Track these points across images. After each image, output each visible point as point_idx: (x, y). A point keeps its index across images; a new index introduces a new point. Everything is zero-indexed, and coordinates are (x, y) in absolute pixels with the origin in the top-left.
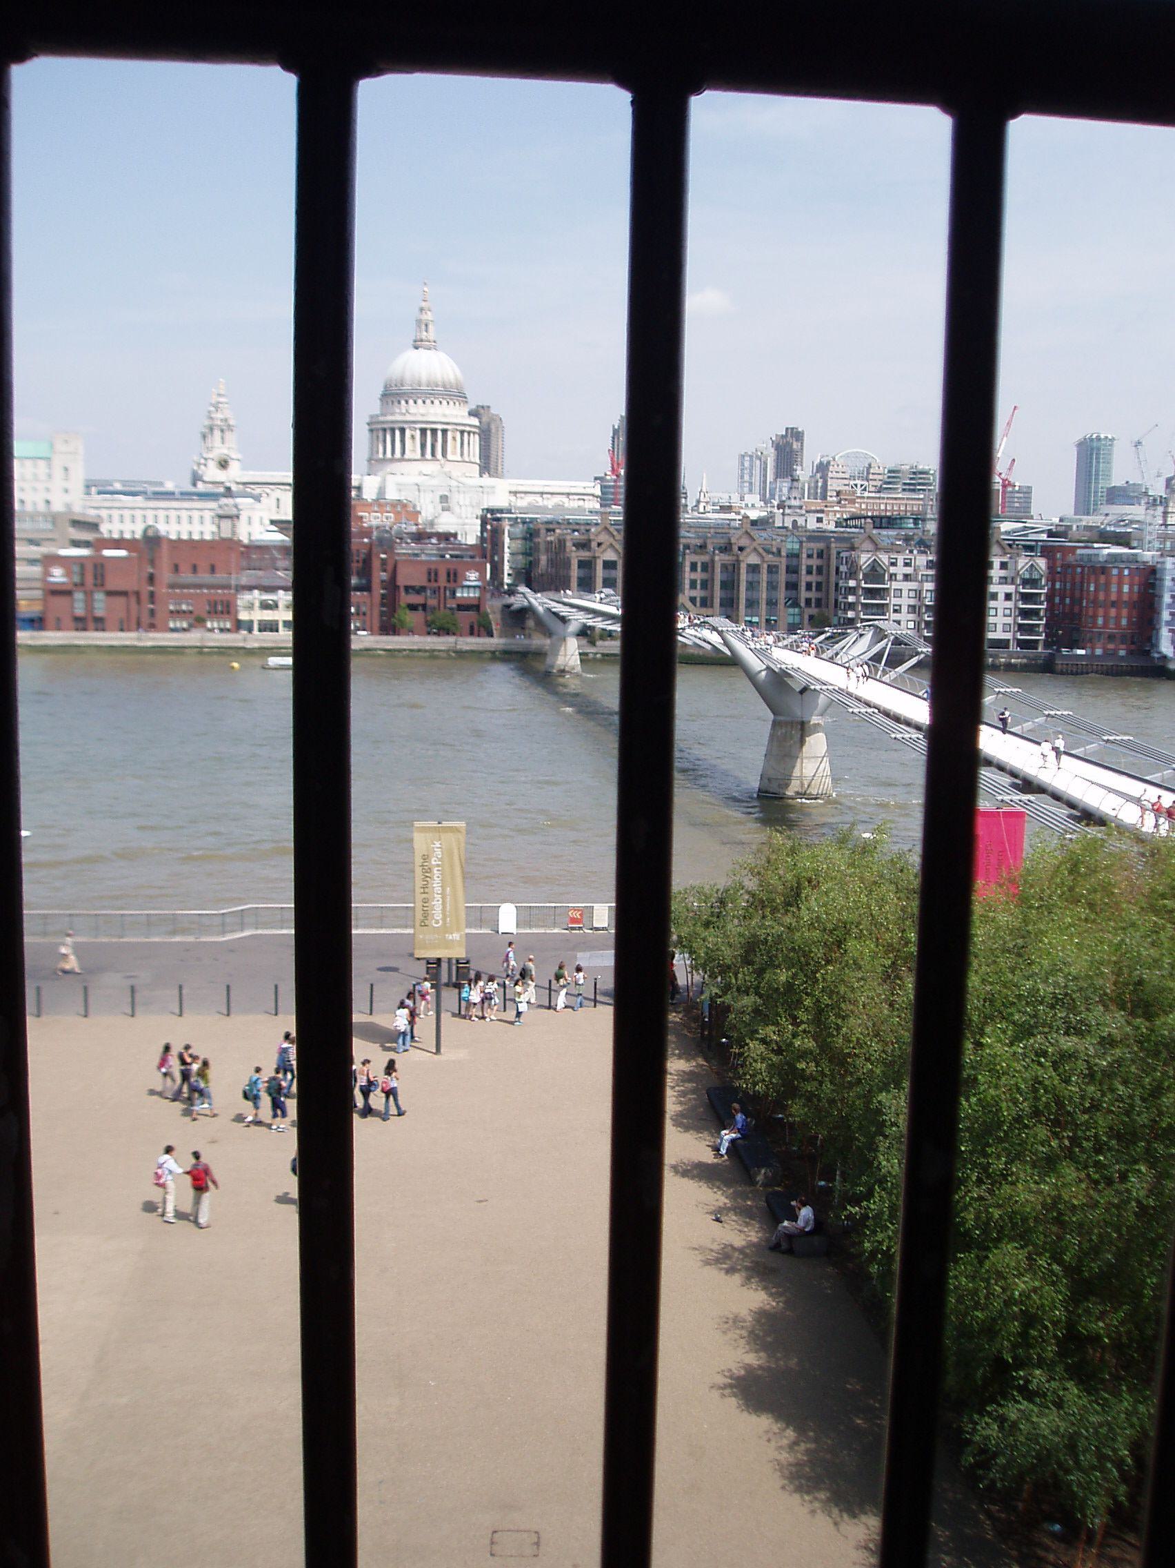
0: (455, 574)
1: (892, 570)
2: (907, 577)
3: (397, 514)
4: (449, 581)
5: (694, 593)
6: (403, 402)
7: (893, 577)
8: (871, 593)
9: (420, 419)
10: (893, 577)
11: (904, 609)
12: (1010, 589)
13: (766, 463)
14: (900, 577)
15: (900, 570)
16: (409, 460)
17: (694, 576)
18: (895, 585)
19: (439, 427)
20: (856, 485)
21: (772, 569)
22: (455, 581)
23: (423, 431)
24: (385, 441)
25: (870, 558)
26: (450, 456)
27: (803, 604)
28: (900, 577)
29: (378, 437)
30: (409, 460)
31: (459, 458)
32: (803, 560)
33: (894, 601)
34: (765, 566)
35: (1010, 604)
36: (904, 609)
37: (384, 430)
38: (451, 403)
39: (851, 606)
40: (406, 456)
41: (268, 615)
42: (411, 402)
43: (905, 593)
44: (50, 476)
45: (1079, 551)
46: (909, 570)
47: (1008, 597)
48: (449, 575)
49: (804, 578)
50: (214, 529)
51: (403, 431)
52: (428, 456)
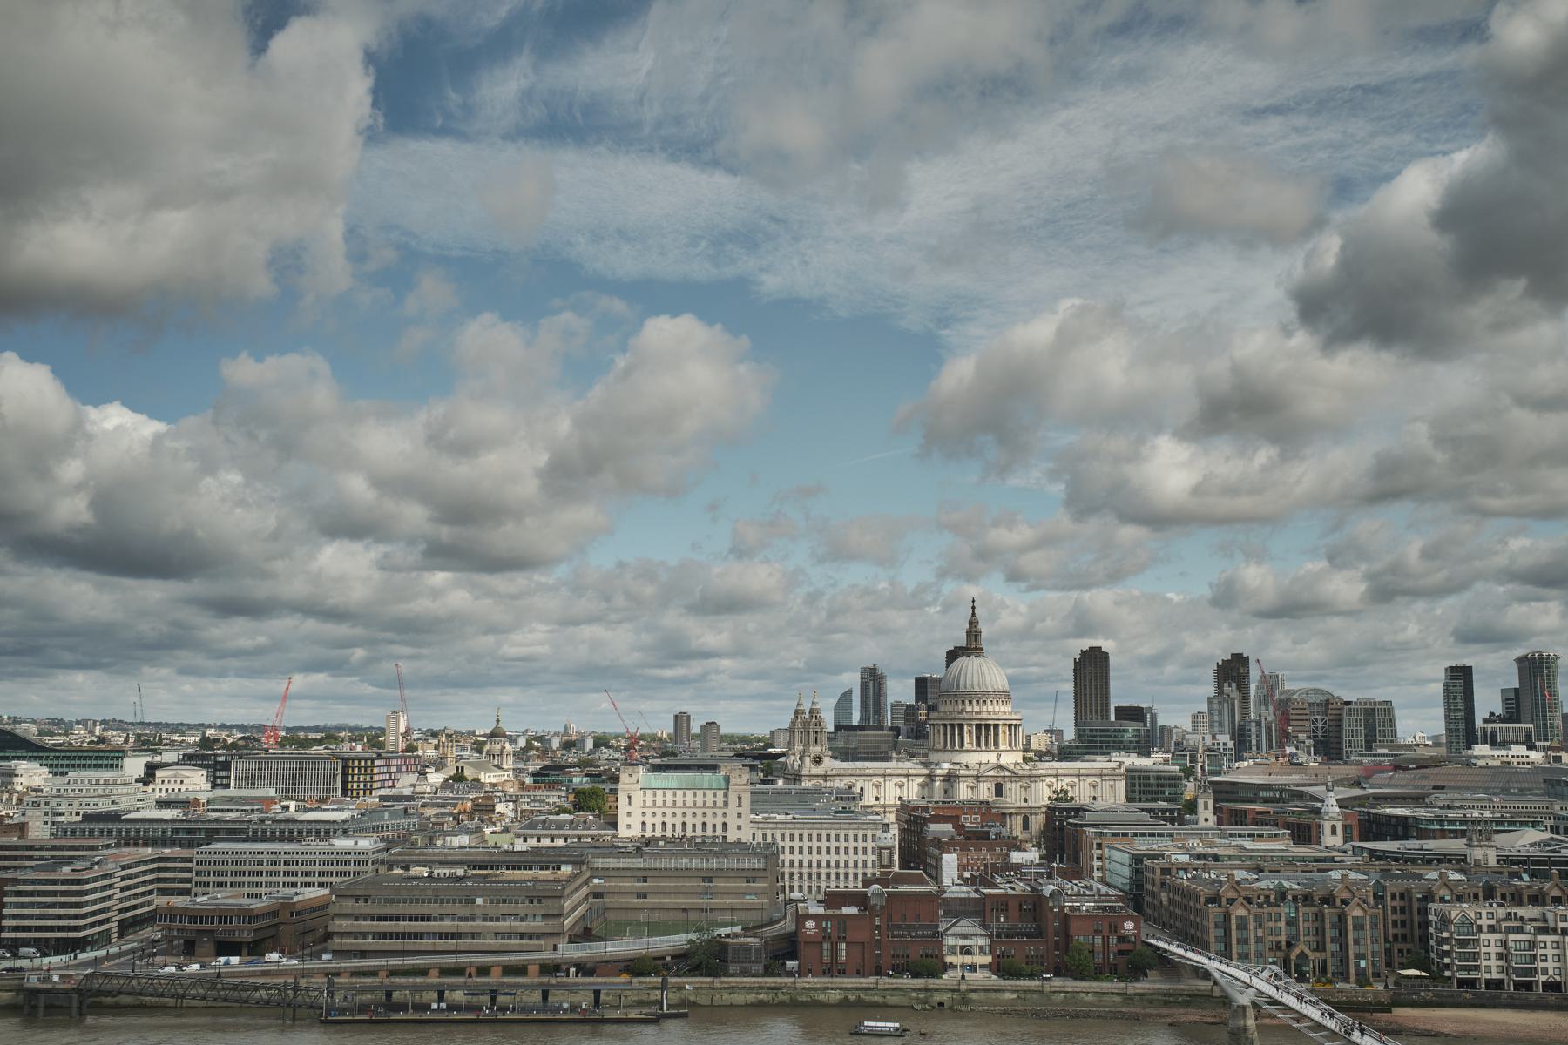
0: (1116, 927)
2: (1492, 929)
3: (983, 815)
4: (1110, 931)
5: (1307, 939)
6: (960, 702)
7: (1480, 928)
9: (975, 716)
13: (1233, 705)
14: (1485, 929)
15: (1485, 922)
16: (967, 751)
18: (1483, 936)
19: (991, 722)
20: (1316, 720)
22: (1116, 932)
23: (978, 727)
24: (945, 734)
25: (1458, 914)
26: (1002, 747)
28: (1485, 929)
29: (939, 731)
30: (967, 751)
31: (1008, 748)
32: (1389, 903)
36: (1493, 956)
37: (945, 725)
38: (1000, 702)
39: (1446, 954)
40: (964, 748)
41: (968, 959)
42: (967, 702)
44: (726, 804)
46: (1493, 922)
48: (1110, 926)
49: (1390, 917)
50: (875, 858)
51: (961, 727)
52: (984, 748)
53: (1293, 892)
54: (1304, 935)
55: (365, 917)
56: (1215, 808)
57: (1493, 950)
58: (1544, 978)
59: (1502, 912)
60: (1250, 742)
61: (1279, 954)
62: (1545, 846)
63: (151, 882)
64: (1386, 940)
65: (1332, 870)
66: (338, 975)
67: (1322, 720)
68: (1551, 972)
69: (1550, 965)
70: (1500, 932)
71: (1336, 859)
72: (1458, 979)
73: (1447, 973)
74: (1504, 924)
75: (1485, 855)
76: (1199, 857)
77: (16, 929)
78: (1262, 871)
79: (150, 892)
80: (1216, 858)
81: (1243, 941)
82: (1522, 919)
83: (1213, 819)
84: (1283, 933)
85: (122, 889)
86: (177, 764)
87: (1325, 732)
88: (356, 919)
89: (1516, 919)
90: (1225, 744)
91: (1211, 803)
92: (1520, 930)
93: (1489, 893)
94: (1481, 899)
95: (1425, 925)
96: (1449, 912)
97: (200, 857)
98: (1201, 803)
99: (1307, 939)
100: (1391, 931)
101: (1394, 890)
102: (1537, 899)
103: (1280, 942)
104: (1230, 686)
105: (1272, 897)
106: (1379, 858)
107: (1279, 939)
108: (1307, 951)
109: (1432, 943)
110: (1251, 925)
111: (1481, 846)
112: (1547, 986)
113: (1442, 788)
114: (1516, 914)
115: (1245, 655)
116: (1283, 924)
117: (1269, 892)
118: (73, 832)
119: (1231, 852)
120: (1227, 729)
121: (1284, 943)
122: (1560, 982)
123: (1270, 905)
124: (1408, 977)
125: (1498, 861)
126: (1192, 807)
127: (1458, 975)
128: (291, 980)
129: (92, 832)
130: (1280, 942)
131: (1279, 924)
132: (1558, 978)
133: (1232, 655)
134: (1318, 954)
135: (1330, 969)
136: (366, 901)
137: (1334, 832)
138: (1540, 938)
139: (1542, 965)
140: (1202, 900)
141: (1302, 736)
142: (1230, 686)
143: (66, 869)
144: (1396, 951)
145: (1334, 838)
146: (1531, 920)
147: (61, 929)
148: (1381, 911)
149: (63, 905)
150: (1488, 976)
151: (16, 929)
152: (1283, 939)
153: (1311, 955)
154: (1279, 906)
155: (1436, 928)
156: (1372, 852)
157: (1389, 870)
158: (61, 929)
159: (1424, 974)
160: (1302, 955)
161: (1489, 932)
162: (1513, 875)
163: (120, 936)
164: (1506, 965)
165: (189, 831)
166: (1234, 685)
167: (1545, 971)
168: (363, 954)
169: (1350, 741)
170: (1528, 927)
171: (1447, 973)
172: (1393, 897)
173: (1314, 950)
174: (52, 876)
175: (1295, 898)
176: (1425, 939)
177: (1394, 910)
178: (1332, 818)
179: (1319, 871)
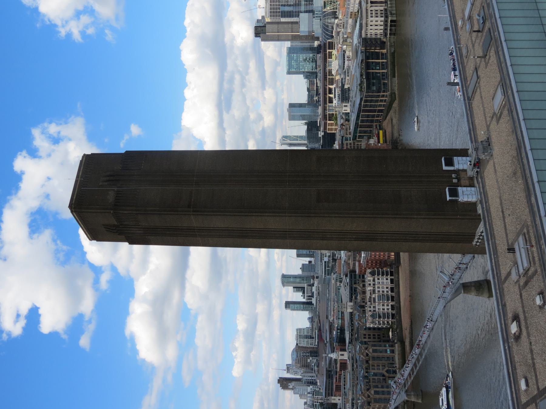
1: (372, 311)
2: (374, 307)
5: (381, 369)
7: (374, 311)
8: (380, 317)
10: (374, 311)
11: (383, 307)
12: (376, 279)
17: (376, 369)
18: (377, 310)
20: (303, 355)
21: (375, 346)
27: (380, 340)
28: (374, 309)
33: (381, 310)
34: (373, 348)
35: (380, 279)
36: (383, 307)
43: (379, 307)
45: (361, 262)
47: (379, 279)
53: (365, 372)
54: (380, 370)
56: (335, 396)
57: (381, 307)
58: (390, 292)
59: (369, 303)
60: (310, 380)
61: (387, 379)
62: (346, 286)
64: (380, 341)
65: (356, 358)
67: (303, 353)
68: (387, 290)
69: (385, 290)
70: (375, 304)
71: (352, 356)
72: (392, 319)
73: (390, 322)
74: (373, 303)
75: (349, 306)
76: (353, 404)
78: (357, 383)
80: (353, 399)
81: (383, 393)
82: (370, 297)
83: (338, 398)
84: (379, 377)
87: (307, 352)
89: (371, 299)
90: (311, 389)
91: (333, 398)
92: (374, 299)
93: (363, 307)
94: (364, 309)
95: (374, 329)
96: (370, 320)
98: (333, 402)
99: (381, 369)
100: (377, 340)
101: (362, 338)
102: (364, 293)
103: (383, 379)
104: (290, 385)
105: (367, 381)
106: (351, 340)
107: (381, 379)
108: (385, 370)
109: (380, 326)
110: (377, 389)
111: (347, 307)
112: (392, 309)
113: (327, 316)
114: (369, 299)
115: (279, 379)
116: (376, 378)
117: (365, 383)
119: (351, 393)
120: (305, 388)
121: (383, 378)
122: (391, 287)
123: (370, 382)
124: (392, 335)
125: (351, 302)
126: (336, 405)
127: (390, 319)
130: (383, 379)
131: (376, 379)
132: (389, 288)
133: (278, 382)
134: (386, 366)
135: (391, 362)
137: (343, 355)
138: (376, 292)
139: (385, 292)
140: (368, 407)
141: (309, 361)
142: (290, 385)
144: (383, 338)
145: (345, 355)
146: (371, 293)
148: (370, 343)
150: (390, 310)
152: (381, 378)
153: (387, 368)
154: (370, 379)
155: (375, 325)
156: (349, 343)
157: (356, 338)
159: (391, 330)
160: (387, 371)
161: (375, 308)
162: (356, 298)
164: (386, 304)
166: (289, 384)
167: (387, 292)
169: (311, 344)
170: (373, 296)
171: (390, 322)
172: (365, 338)
173: (385, 367)
175: (367, 372)
176: (379, 329)
177: (369, 338)
178: (338, 355)
179: (357, 362)
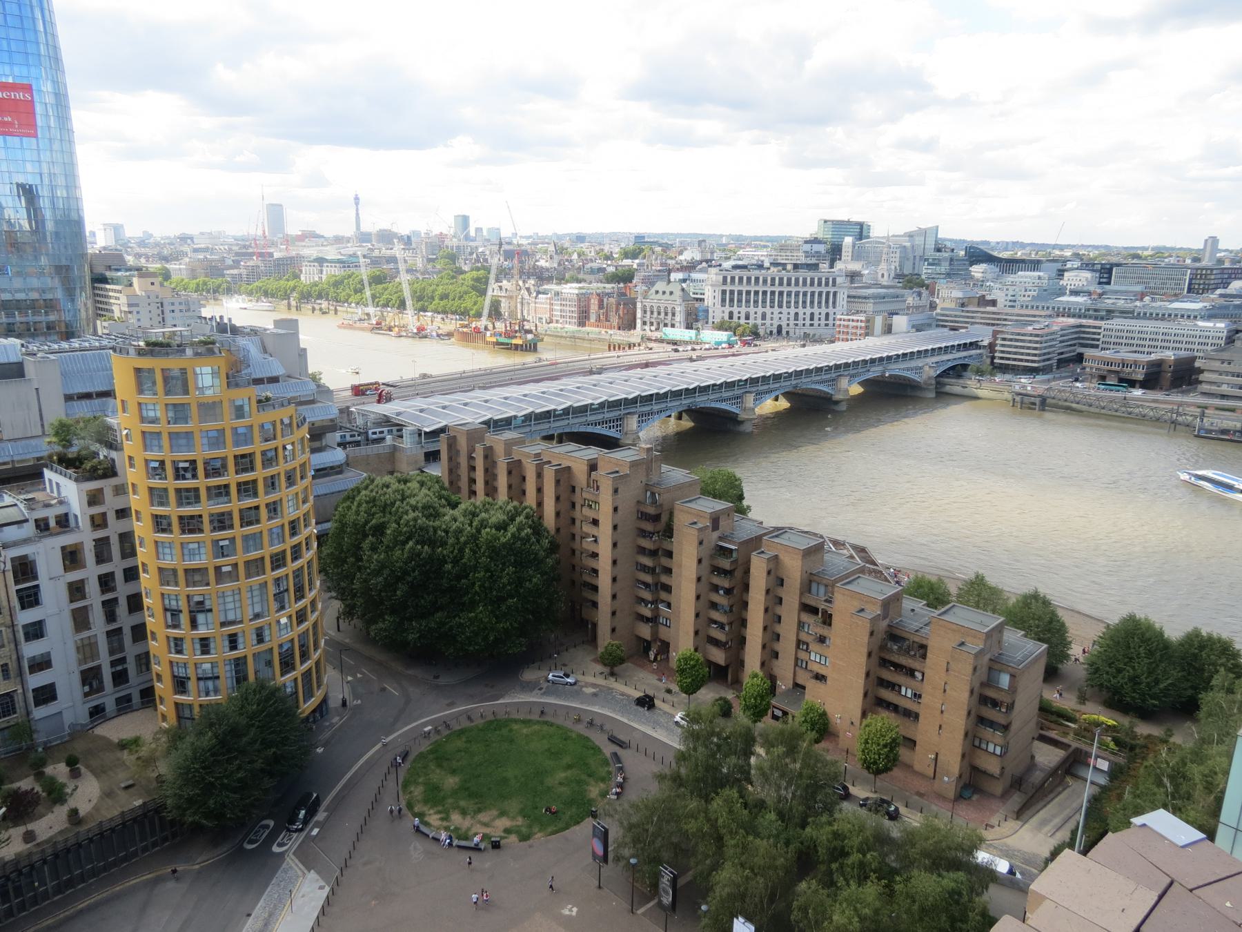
55: (1227, 373)
63: (1075, 339)
66: (1206, 408)
77: (1002, 358)
79: (1075, 345)
85: (1061, 342)
86: (1077, 269)
88: (1221, 374)
97: (1106, 326)
118: (1027, 307)
128: (1176, 407)
129: (1037, 307)
136: (1229, 363)
143: (1030, 328)
147: (1027, 361)
149: (1029, 348)
151: (1002, 358)
158: (1027, 361)
163: (1058, 367)
165: (1096, 310)
168: (1223, 397)
174: (1023, 331)
